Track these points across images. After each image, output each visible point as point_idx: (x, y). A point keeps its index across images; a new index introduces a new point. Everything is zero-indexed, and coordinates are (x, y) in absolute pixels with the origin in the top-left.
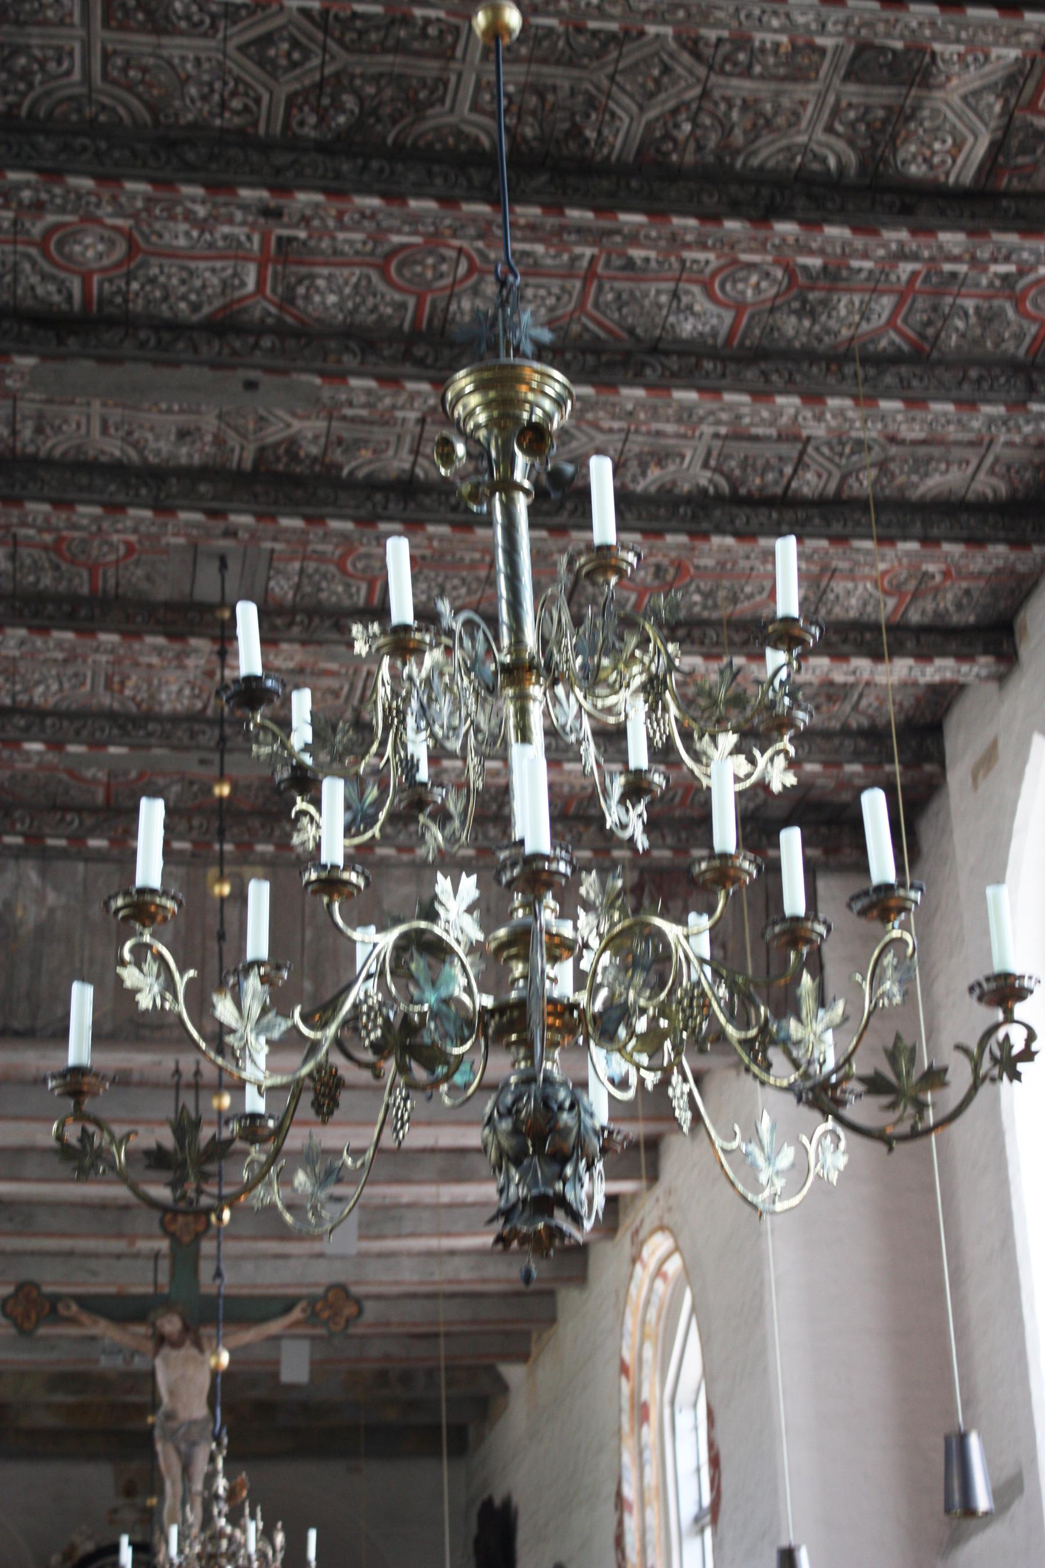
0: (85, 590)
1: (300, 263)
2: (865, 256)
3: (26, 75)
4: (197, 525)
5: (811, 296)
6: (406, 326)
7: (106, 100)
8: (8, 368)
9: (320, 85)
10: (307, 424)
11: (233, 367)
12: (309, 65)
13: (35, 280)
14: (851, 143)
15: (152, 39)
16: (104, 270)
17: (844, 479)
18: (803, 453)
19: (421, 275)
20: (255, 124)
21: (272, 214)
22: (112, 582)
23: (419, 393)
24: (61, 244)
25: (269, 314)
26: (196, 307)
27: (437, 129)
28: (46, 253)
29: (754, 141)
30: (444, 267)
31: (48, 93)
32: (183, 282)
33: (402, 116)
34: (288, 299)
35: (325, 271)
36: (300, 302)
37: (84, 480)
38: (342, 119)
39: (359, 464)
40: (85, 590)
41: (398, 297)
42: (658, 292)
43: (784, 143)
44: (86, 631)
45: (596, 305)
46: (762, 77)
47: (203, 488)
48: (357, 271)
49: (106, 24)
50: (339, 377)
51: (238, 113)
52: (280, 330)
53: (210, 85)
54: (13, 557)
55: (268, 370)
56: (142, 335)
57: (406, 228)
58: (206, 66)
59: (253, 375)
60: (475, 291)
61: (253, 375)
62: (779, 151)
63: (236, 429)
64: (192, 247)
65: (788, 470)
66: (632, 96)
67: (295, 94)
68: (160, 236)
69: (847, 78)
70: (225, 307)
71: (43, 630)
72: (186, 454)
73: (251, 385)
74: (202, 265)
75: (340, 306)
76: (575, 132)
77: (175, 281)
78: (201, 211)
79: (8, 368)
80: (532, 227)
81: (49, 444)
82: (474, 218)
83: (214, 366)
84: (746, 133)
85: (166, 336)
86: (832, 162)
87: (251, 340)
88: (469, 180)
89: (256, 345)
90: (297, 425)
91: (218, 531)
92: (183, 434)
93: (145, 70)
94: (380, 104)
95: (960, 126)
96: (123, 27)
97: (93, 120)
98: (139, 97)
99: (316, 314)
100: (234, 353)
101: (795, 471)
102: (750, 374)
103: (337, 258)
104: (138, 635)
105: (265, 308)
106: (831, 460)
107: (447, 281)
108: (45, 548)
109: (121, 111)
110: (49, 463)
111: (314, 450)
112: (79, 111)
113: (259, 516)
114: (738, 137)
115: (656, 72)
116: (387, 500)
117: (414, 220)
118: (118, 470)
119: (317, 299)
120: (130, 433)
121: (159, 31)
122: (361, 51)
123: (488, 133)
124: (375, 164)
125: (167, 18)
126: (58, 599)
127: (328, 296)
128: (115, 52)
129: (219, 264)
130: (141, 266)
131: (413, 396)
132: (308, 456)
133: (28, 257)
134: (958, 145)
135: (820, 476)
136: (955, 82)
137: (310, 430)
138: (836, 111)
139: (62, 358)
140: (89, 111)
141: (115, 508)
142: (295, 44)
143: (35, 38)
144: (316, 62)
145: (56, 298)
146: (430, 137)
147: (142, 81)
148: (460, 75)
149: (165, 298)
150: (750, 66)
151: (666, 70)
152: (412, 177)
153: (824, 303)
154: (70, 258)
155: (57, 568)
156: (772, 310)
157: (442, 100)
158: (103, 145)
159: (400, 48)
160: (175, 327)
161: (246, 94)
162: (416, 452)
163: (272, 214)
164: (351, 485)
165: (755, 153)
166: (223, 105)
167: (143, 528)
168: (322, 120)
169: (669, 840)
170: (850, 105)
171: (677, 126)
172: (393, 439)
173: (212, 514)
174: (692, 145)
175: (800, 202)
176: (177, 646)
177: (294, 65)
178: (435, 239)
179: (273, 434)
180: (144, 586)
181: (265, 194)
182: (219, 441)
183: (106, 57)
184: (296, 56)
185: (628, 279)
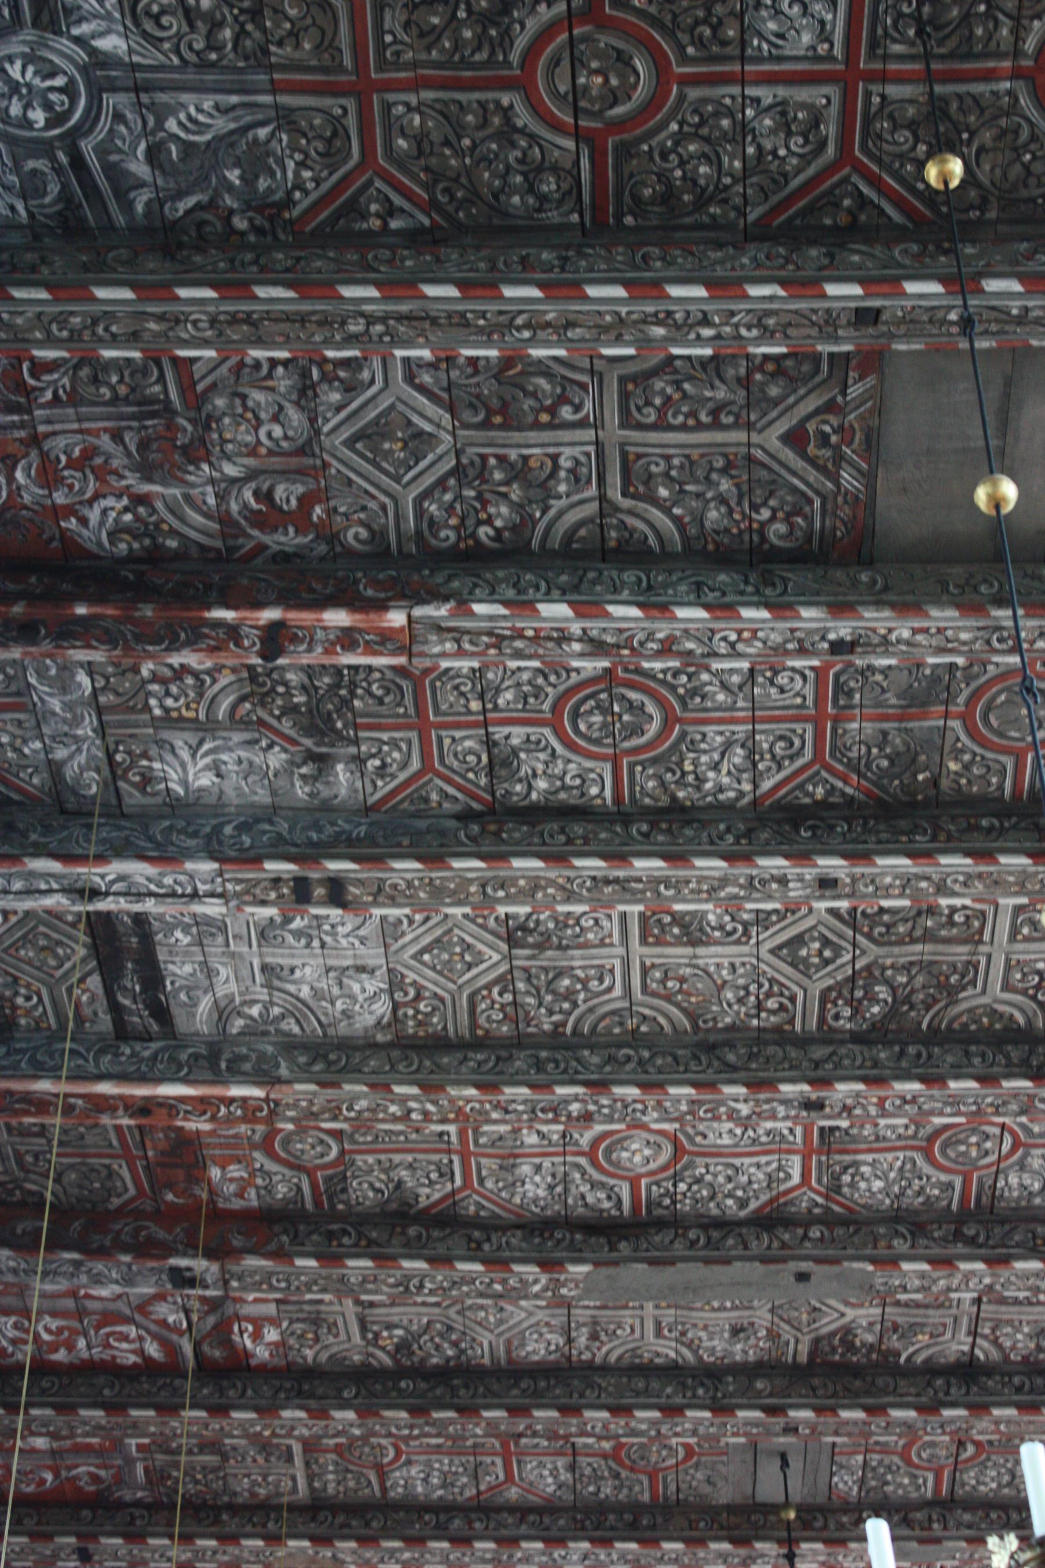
0: (646, 1497)
3: (569, 995)
4: (756, 1424)
6: (954, 1207)
7: (647, 1012)
8: (562, 1277)
9: (853, 979)
10: (862, 1312)
11: (783, 1260)
12: (839, 962)
13: (585, 1188)
15: (689, 951)
19: (964, 1154)
20: (792, 1021)
21: (815, 1106)
22: (673, 1487)
23: (973, 1273)
24: (609, 1151)
25: (817, 1205)
26: (743, 1203)
27: (970, 1011)
28: (595, 1163)
30: (988, 1145)
31: (591, 1010)
32: (729, 1179)
33: (936, 1001)
34: (835, 1187)
35: (869, 1157)
36: (846, 1190)
38: (876, 1009)
39: (918, 1349)
40: (646, 1497)
41: (944, 1178)
44: (650, 1541)
47: (759, 1385)
48: (901, 1155)
49: (644, 941)
50: (892, 1262)
51: (773, 1012)
52: (828, 1220)
53: (746, 988)
54: (572, 1468)
55: (819, 1261)
56: (692, 1235)
57: (948, 1110)
58: (741, 971)
59: (805, 1266)
60: (1022, 1166)
61: (805, 1266)
63: (788, 1322)
64: (736, 1145)
67: (829, 989)
68: (705, 1137)
70: (771, 1201)
71: (606, 1542)
72: (740, 1351)
73: (802, 1277)
74: (747, 1161)
75: (886, 1191)
77: (721, 1179)
78: (745, 1109)
79: (562, 1277)
81: (604, 1349)
82: (1015, 1095)
83: (765, 1260)
85: (715, 1234)
87: (800, 1231)
88: (1007, 1057)
89: (805, 1236)
90: (851, 1313)
91: (778, 1428)
92: (736, 1331)
93: (682, 980)
94: (913, 991)
96: (659, 942)
97: (635, 1031)
98: (678, 1005)
99: (862, 1201)
100: (784, 1246)
103: (879, 1144)
104: (702, 1542)
105: (810, 1199)
107: (992, 1158)
108: (605, 1456)
109: (662, 1020)
110: (604, 1369)
111: (870, 1338)
112: (621, 1024)
113: (819, 1410)
116: (949, 1385)
117: (955, 1101)
118: (673, 1371)
119: (863, 1185)
120: (683, 1334)
121: (694, 943)
122: (891, 944)
123: (1022, 1011)
124: (912, 1050)
125: (701, 930)
126: (620, 1509)
127: (873, 1183)
128: (653, 966)
129: (763, 1159)
130: (685, 1168)
131: (968, 1276)
132: (863, 1344)
133: (578, 1166)
137: (863, 1317)
139: (615, 1263)
140: (630, 1024)
141: (673, 1411)
142: (826, 942)
143: (577, 959)
144: (847, 957)
145: (606, 1205)
146: (964, 1019)
147: (680, 991)
148: (989, 957)
149: (712, 1197)
152: (950, 1059)
154: (617, 1164)
155: (617, 1476)
157: (973, 983)
158: (646, 1054)
159: (928, 937)
160: (724, 1224)
161: (782, 995)
162: (974, 1333)
163: (815, 1106)
164: (910, 1371)
166: (759, 1006)
167: (701, 1430)
168: (856, 1012)
172: (949, 1321)
173: (771, 1411)
176: (743, 1552)
177: (827, 962)
178: (978, 1115)
179: (828, 1324)
180: (707, 1489)
181: (806, 1088)
182: (773, 1335)
183: (645, 971)
184: (827, 953)
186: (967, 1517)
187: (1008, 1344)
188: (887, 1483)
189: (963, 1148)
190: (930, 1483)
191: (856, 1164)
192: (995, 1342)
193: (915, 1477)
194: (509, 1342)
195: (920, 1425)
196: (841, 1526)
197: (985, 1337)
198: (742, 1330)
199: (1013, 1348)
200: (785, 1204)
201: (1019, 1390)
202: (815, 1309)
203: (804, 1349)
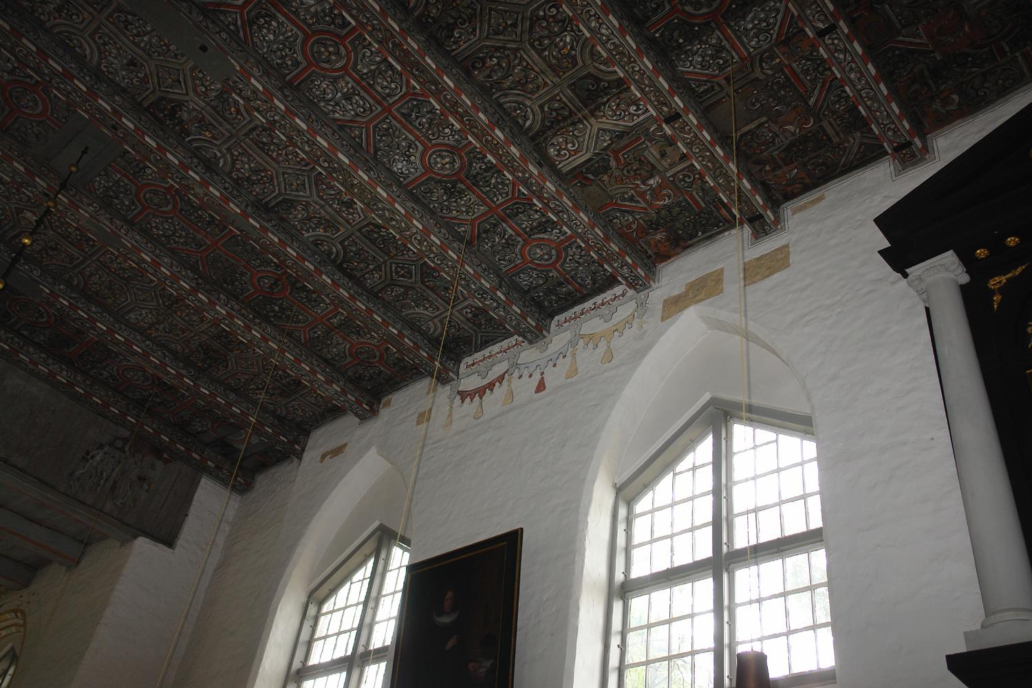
2: (512, 174)
6: (288, 78)
14: (543, 120)
17: (389, 285)
18: (385, 262)
19: (320, 53)
22: (17, 126)
25: (235, 24)
29: (512, 89)
34: (251, 23)
35: (281, 18)
37: (61, 52)
42: (405, 139)
43: (520, 99)
45: (375, 127)
46: (544, 59)
47: (117, 98)
48: (295, 29)
62: (515, 102)
65: (371, 267)
66: (489, 26)
69: (569, 86)
76: (451, 28)
80: (407, 53)
81: (58, 21)
82: (388, 30)
84: (513, 82)
86: (528, 123)
87: (218, 30)
89: (219, 33)
95: (586, 143)
100: (207, 27)
101: (372, 270)
102: (409, 204)
111: (185, 116)
114: (507, 83)
115: (509, 23)
116: (199, 164)
120: (105, 44)
132: (180, 117)
134: (576, 152)
135: (381, 277)
136: (604, 119)
138: (552, 99)
150: (545, 50)
151: (514, 25)
153: (461, 192)
156: (439, 182)
165: (506, 95)
169: (154, 426)
170: (560, 100)
171: (491, 58)
172: (228, 134)
174: (487, 72)
175: (507, 130)
182: (144, 81)
185: (400, 122)
186: (138, 237)
188: (117, 198)
189: (323, 50)
191: (274, 17)
192: (234, 163)
193: (133, 203)
196: (82, 201)
197: (232, 155)
198: (135, 65)
199: (238, 170)
200: (221, 12)
201: (226, 189)
203: (152, 98)
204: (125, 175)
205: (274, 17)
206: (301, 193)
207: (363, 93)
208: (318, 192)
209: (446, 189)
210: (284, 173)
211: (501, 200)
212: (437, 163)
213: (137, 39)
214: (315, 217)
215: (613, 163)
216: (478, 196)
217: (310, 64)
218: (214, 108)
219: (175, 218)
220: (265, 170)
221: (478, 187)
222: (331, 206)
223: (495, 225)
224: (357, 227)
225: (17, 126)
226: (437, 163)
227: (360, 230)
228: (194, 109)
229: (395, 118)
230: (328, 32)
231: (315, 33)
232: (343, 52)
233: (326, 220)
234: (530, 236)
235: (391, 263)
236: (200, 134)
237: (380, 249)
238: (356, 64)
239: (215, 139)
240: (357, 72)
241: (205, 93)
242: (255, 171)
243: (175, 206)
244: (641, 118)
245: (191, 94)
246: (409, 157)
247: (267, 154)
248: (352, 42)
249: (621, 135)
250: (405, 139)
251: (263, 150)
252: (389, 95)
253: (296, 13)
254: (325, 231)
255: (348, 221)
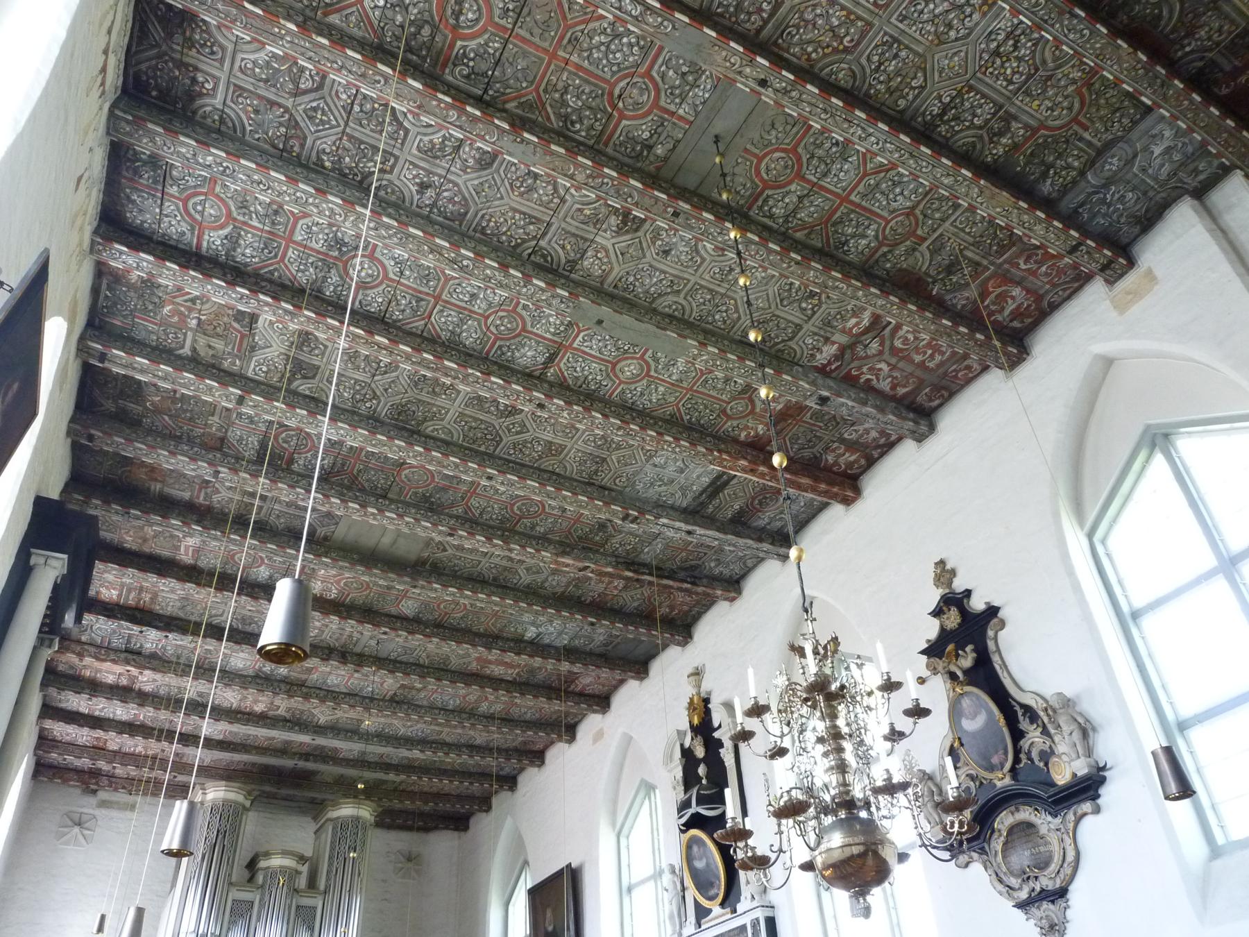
1: (555, 342)
5: (336, 253)
10: (604, 242)
16: (632, 358)
18: (346, 124)
19: (510, 323)
22: (795, 130)
35: (548, 336)
41: (524, 313)
42: (409, 278)
45: (439, 280)
65: (357, 108)
69: (319, 367)
80: (447, 375)
101: (352, 104)
106: (330, 109)
107: (500, 314)
129: (587, 350)
138: (323, 354)
151: (386, 390)
153: (330, 247)
159: (476, 419)
162: (563, 200)
172: (568, 220)
185: (420, 292)
187: (550, 187)
188: (684, 74)
190: (660, 60)
191: (554, 334)
194: (766, 284)
195: (612, 192)
202: (622, 254)
204: (673, 114)
205: (554, 334)
206: (476, 182)
207: (463, 304)
208: (460, 191)
209: (345, 244)
210: (502, 198)
211: (290, 253)
212: (370, 268)
213: (662, 276)
214: (450, 154)
215: (236, 325)
216: (312, 249)
217: (514, 310)
218: (586, 240)
219: (608, 76)
220: (521, 195)
221: (320, 260)
222: (440, 176)
223: (273, 223)
224: (401, 162)
225: (795, 130)
226: (370, 268)
227: (397, 158)
228: (605, 231)
229: (428, 294)
230: (509, 339)
231: (519, 335)
232: (492, 328)
233: (436, 157)
234: (235, 227)
235: (339, 125)
236: (595, 209)
237: (362, 142)
238: (479, 324)
239: (579, 210)
240: (475, 320)
241: (597, 252)
242: (531, 189)
243: (611, 94)
244: (252, 366)
245: (610, 247)
246: (397, 263)
247: (524, 214)
248: (489, 338)
249: (253, 349)
250: (409, 278)
251: (530, 216)
252: (442, 311)
253: (538, 343)
254: (431, 141)
255: (416, 166)
